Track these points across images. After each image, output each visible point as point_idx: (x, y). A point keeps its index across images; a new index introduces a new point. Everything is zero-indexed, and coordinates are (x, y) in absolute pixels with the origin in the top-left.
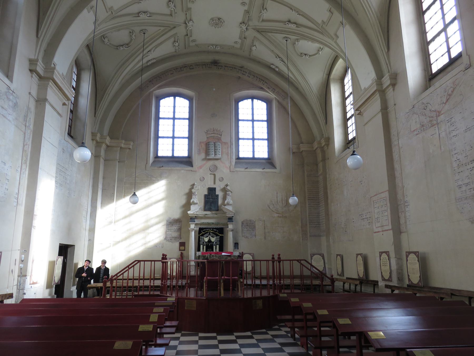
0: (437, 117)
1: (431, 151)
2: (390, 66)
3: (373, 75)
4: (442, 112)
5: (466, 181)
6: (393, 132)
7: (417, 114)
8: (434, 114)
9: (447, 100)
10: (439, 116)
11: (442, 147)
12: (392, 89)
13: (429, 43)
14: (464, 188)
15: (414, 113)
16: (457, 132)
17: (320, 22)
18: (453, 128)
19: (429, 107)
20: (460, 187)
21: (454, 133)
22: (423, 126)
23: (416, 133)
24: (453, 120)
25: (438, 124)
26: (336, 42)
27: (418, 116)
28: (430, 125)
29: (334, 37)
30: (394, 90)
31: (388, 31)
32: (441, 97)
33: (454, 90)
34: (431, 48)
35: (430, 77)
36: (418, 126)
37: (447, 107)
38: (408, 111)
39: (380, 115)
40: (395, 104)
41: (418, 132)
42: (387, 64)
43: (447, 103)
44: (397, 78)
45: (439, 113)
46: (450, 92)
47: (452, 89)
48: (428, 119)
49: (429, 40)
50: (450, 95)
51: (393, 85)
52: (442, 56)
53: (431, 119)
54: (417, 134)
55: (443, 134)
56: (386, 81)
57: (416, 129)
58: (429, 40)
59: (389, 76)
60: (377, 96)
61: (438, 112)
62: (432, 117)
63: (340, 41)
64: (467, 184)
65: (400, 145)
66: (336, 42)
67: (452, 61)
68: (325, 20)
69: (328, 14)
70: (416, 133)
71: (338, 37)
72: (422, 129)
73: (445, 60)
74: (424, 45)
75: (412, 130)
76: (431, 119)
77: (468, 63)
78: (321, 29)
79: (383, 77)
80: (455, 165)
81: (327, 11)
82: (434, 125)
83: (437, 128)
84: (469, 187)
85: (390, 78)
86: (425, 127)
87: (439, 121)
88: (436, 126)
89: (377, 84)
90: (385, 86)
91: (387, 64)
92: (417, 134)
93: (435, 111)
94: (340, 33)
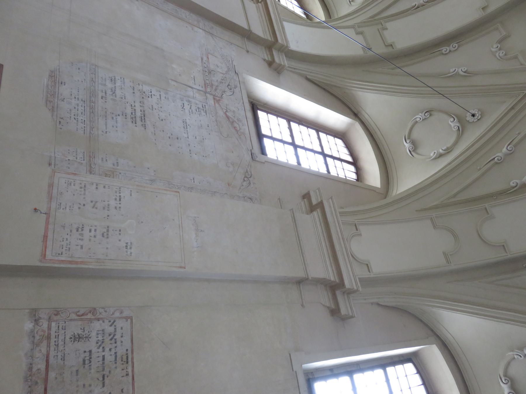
0: (214, 96)
1: (174, 66)
2: (291, 71)
3: (293, 46)
4: (217, 105)
5: (118, 92)
6: (217, 30)
7: (226, 73)
8: (218, 93)
9: (228, 117)
10: (214, 99)
11: (175, 83)
12: (267, 59)
13: (289, 121)
14: (109, 85)
15: (229, 69)
16: (187, 111)
17: (388, 25)
18: (193, 108)
19: (229, 93)
20: (113, 80)
21: (187, 107)
22: (210, 73)
23: (205, 59)
24: (203, 113)
25: (206, 92)
26: (352, 27)
27: (224, 72)
28: (208, 82)
29: (361, 30)
30: (265, 60)
31: (324, 89)
32: (234, 112)
33: (236, 130)
34: (283, 122)
35: (256, 106)
36: (212, 67)
37: (221, 113)
38: (234, 63)
39: (245, 26)
40: (248, 52)
41: (204, 61)
42: (295, 69)
43: (224, 116)
44: (275, 72)
45: (217, 100)
46: (236, 125)
47: (238, 129)
48: (216, 84)
49: (292, 123)
50: (232, 123)
51: (270, 64)
52: (271, 129)
53: (214, 87)
54: (202, 59)
55: (190, 92)
56: (279, 59)
57: (208, 61)
58: (292, 123)
59: (284, 66)
60: (268, 37)
61: (219, 100)
62: (216, 90)
63: (351, 32)
64: (114, 92)
65: (196, 29)
66: (352, 27)
67: (260, 137)
68: (385, 33)
69: (389, 41)
70: (205, 59)
71: (357, 33)
72: (207, 70)
73: (265, 131)
74: (290, 117)
75: (210, 56)
76: (214, 87)
77: (257, 159)
78: (378, 21)
79: (286, 56)
80: (146, 88)
81: (393, 43)
82: (205, 87)
83: (200, 88)
84: (109, 92)
85: (280, 65)
86: (207, 74)
87: (208, 95)
88: (203, 89)
89: (283, 46)
90: (275, 53)
91: (295, 69)
92: (202, 59)
93: (221, 97)
94: (360, 38)
